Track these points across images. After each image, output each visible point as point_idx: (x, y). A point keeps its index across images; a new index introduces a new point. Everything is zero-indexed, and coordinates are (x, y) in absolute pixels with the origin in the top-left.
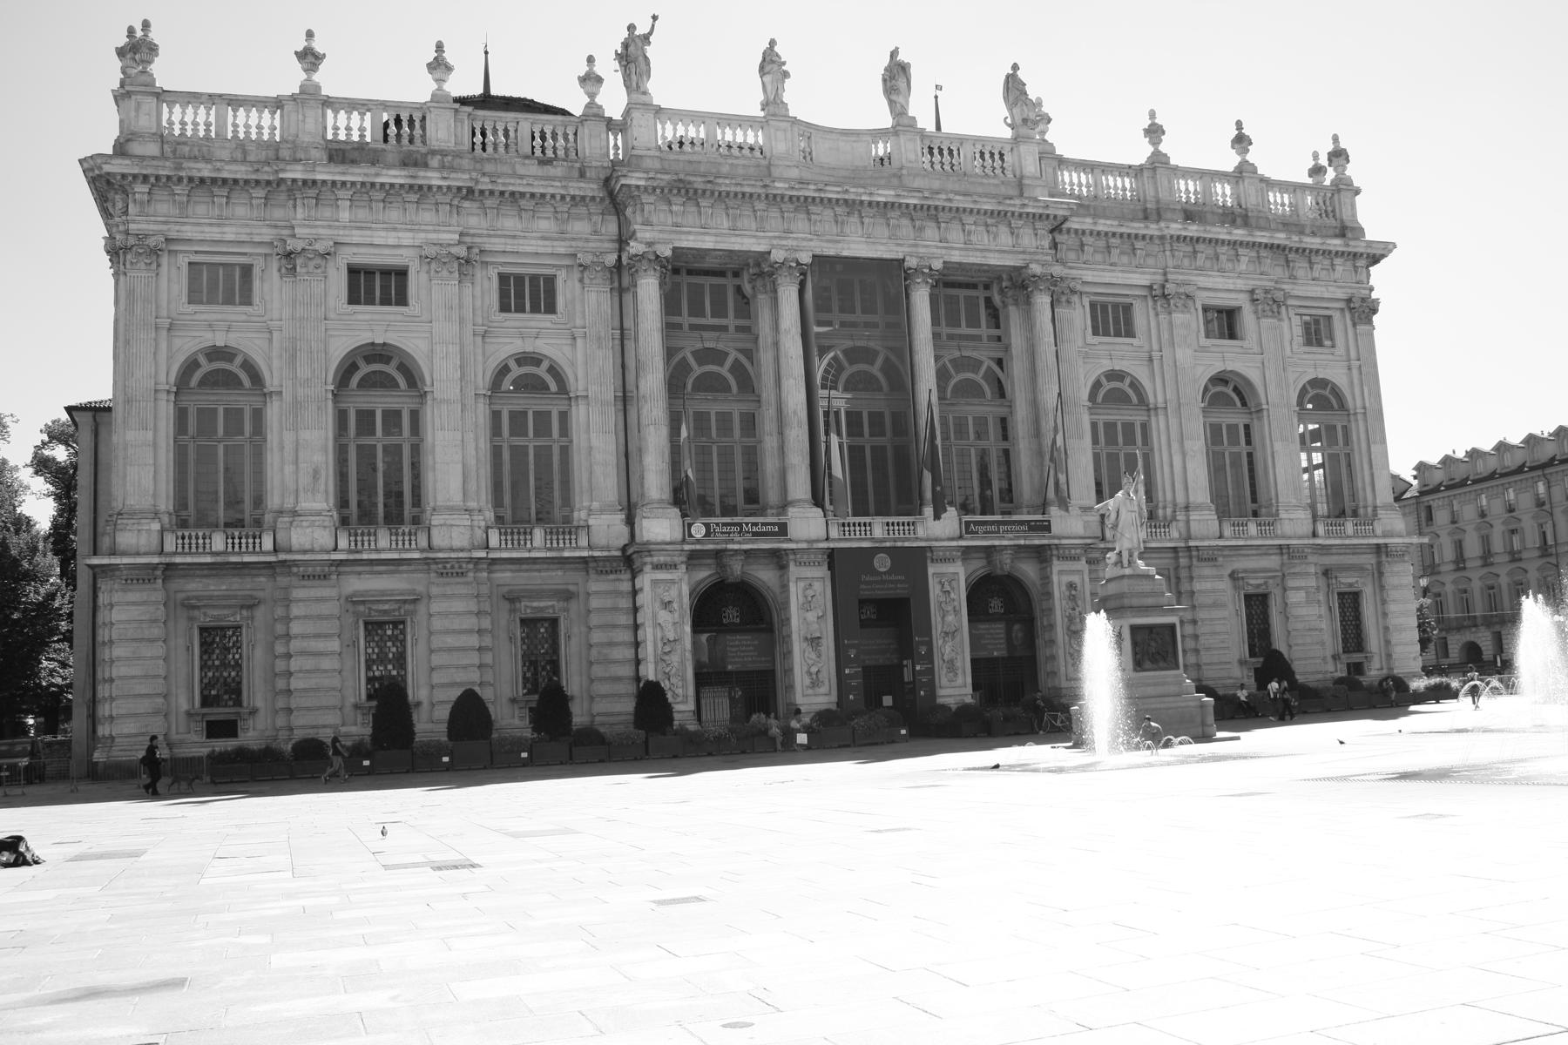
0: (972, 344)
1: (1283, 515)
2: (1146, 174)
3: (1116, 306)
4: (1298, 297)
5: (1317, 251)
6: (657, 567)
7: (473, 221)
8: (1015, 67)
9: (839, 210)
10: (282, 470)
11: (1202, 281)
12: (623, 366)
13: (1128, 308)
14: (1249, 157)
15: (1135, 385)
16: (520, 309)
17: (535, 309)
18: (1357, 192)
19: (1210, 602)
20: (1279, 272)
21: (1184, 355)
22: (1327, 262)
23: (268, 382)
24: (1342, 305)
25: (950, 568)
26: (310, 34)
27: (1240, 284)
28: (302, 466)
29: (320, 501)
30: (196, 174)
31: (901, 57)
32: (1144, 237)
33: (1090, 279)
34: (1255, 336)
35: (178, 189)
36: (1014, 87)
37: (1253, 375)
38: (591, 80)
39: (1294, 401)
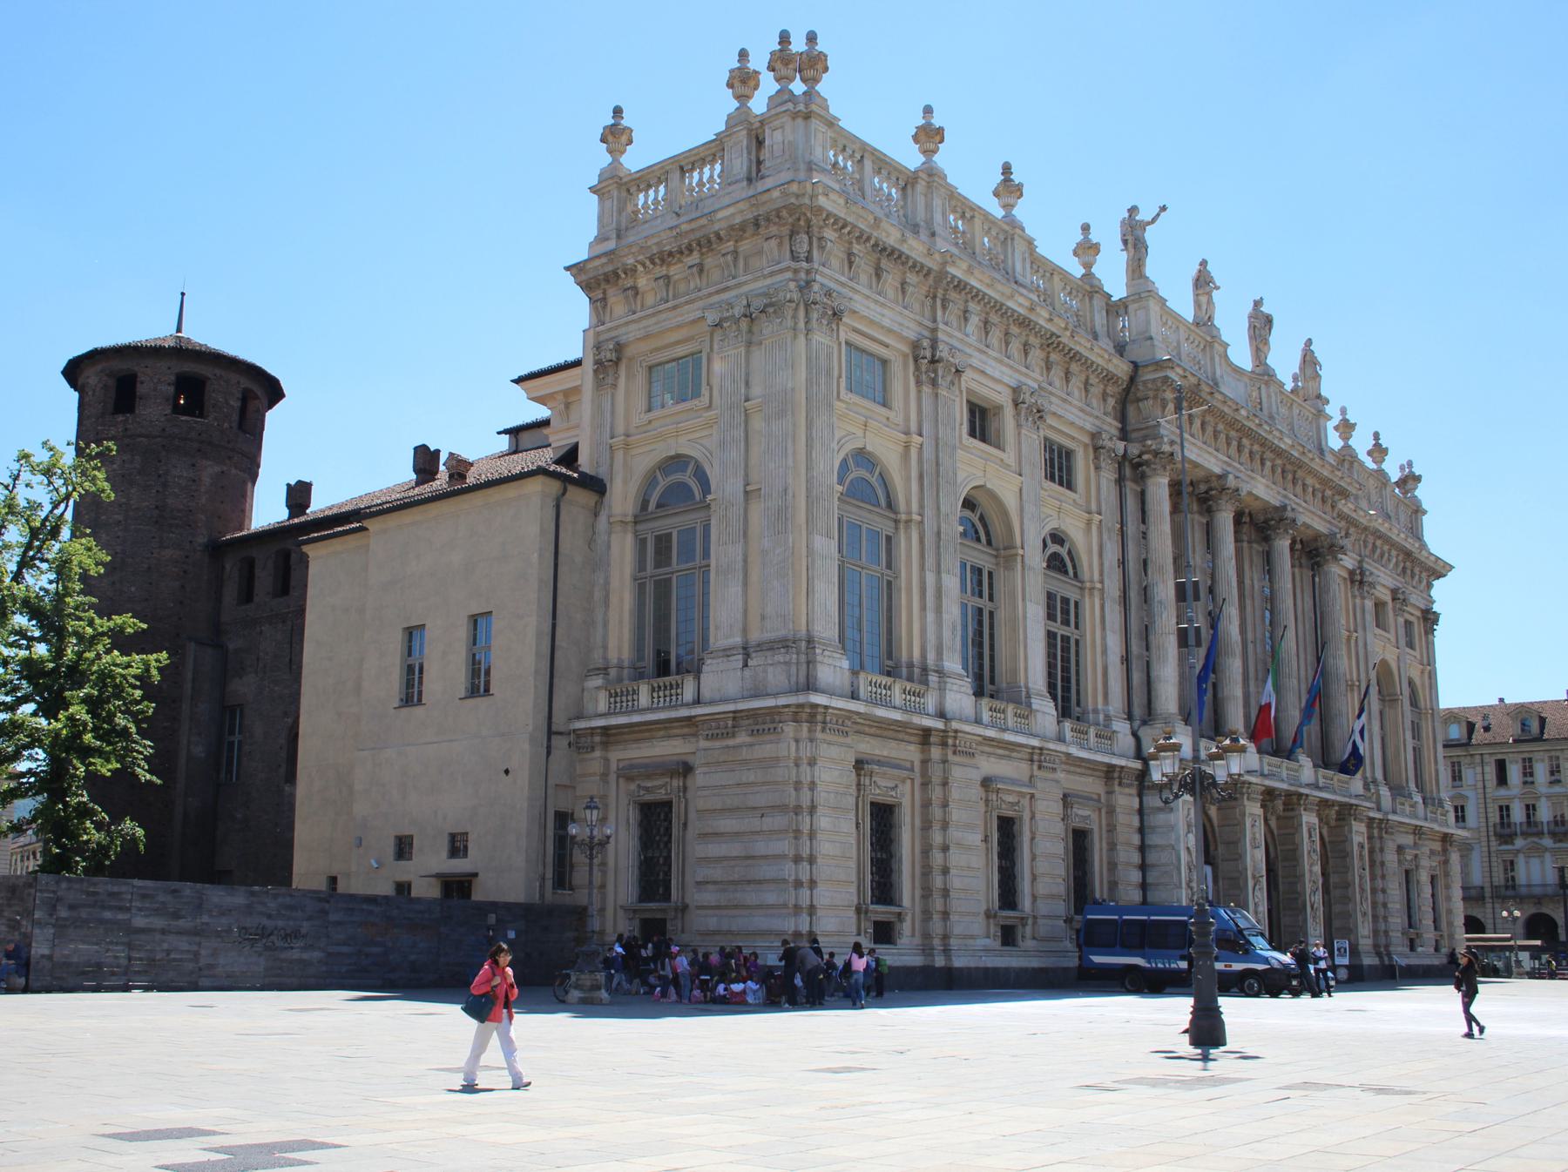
2: (1346, 465)
8: (1309, 342)
10: (923, 618)
12: (1123, 563)
14: (1384, 466)
17: (1061, 484)
18: (1425, 512)
21: (1370, 637)
23: (902, 507)
24: (1418, 614)
26: (928, 110)
27: (1391, 583)
28: (945, 616)
29: (953, 664)
30: (883, 236)
31: (1265, 309)
34: (1392, 630)
35: (856, 248)
36: (1309, 362)
37: (1394, 665)
38: (1087, 250)
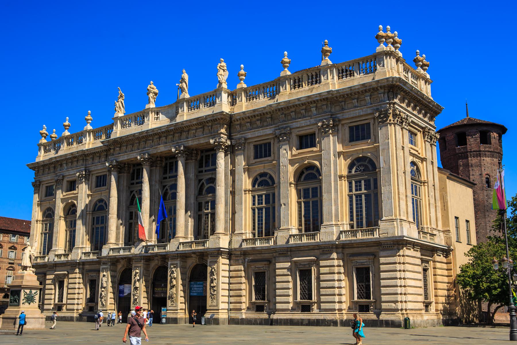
0: (211, 172)
1: (322, 230)
3: (265, 144)
4: (348, 119)
5: (351, 94)
6: (104, 264)
7: (90, 162)
9: (156, 137)
11: (295, 125)
13: (270, 144)
15: (271, 178)
16: (100, 186)
17: (103, 186)
19: (282, 273)
20: (338, 108)
22: (363, 96)
25: (176, 262)
32: (267, 113)
33: (250, 136)
37: (317, 163)
39: (345, 172)
